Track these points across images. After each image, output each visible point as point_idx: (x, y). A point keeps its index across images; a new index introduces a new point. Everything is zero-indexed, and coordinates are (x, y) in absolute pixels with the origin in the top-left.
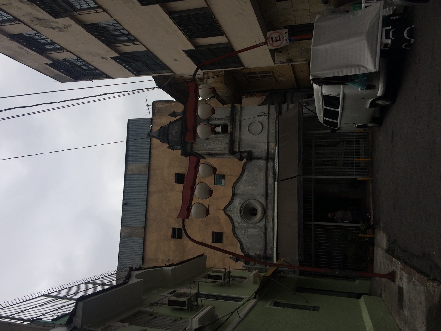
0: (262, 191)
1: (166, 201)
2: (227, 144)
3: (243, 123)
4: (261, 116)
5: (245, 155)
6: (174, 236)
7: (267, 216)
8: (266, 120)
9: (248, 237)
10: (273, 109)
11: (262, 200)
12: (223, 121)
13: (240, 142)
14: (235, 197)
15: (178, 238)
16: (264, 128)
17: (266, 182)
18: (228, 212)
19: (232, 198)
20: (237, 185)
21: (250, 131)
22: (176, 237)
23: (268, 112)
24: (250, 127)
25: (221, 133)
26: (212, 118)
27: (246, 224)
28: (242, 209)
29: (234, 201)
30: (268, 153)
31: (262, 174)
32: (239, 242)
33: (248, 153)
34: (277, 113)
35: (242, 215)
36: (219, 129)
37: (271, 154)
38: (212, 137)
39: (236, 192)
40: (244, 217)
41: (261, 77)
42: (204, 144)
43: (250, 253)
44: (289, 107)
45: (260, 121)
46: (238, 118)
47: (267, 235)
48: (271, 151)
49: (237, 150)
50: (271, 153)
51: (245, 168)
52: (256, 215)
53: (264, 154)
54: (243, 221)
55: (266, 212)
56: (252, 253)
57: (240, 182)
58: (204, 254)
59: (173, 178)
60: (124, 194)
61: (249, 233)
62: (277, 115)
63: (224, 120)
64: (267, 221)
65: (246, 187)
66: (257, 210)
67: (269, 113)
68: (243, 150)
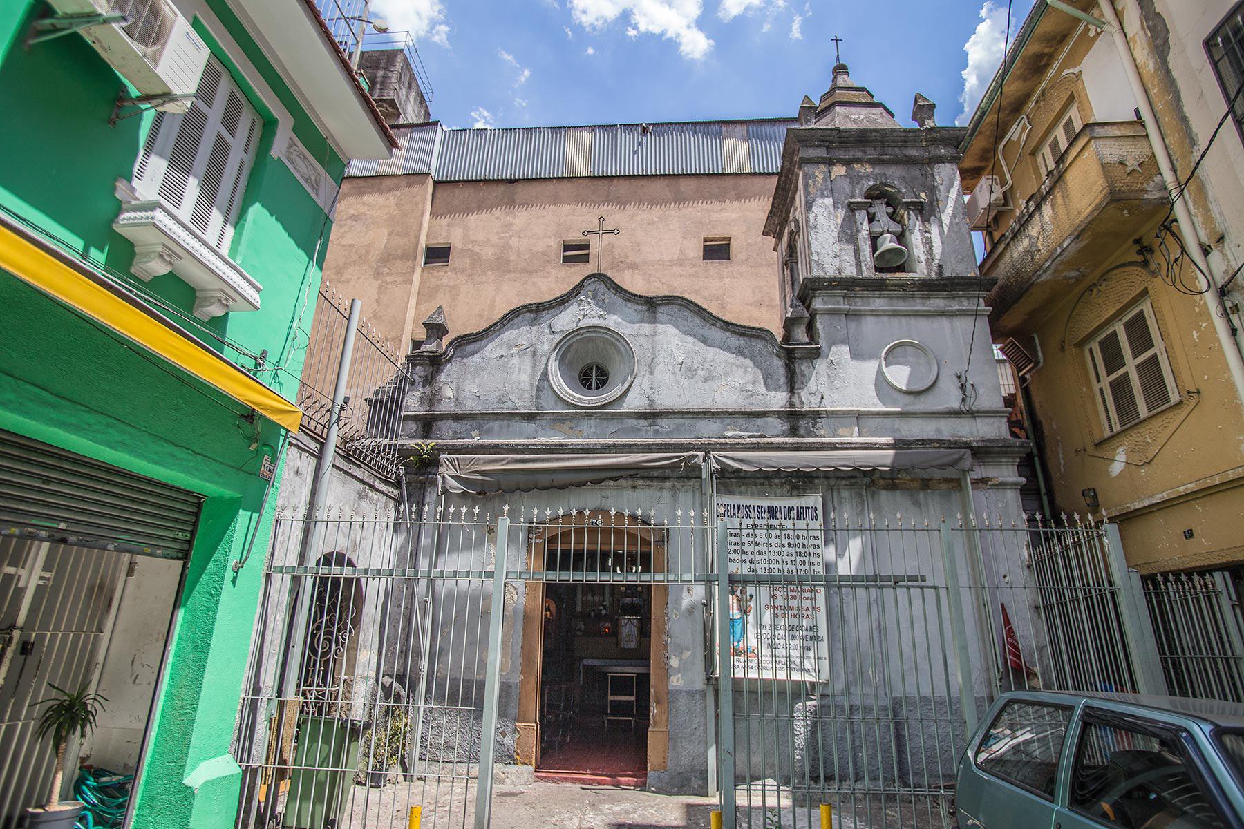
0: (666, 401)
1: (656, 220)
2: (837, 272)
3: (923, 323)
4: (963, 387)
5: (801, 334)
6: (567, 247)
7: (571, 417)
8: (945, 406)
9: (502, 356)
10: (995, 429)
11: (635, 402)
12: (923, 258)
13: (848, 314)
14: (645, 308)
15: (564, 256)
16: (912, 397)
17: (704, 413)
18: (590, 288)
19: (641, 297)
20: (687, 314)
21: (895, 351)
22: (567, 254)
23: (978, 412)
24: (909, 349)
25: (876, 254)
26: (928, 221)
27: (546, 347)
28: (600, 332)
29: (630, 305)
30: (816, 415)
31: (734, 398)
32: (487, 329)
33: (807, 344)
34: (980, 444)
35: (578, 334)
36: (888, 243)
37: (813, 427)
38: (859, 223)
39: (661, 309)
40: (574, 340)
41: (1121, 388)
42: (829, 197)
43: (449, 366)
44: (1009, 491)
45: (940, 384)
46: (937, 303)
47: (505, 423)
48: (823, 426)
49: (818, 304)
50: (819, 425)
51: (752, 336)
52: (584, 385)
53: (808, 400)
54: (558, 338)
55: (589, 416)
56: (450, 372)
57: (698, 320)
58: (400, 149)
59: (718, 232)
60: (671, 124)
61: (516, 360)
62: (975, 444)
63: (927, 261)
64: (559, 419)
65: (680, 343)
66: (598, 388)
67: (973, 414)
68: (818, 325)
